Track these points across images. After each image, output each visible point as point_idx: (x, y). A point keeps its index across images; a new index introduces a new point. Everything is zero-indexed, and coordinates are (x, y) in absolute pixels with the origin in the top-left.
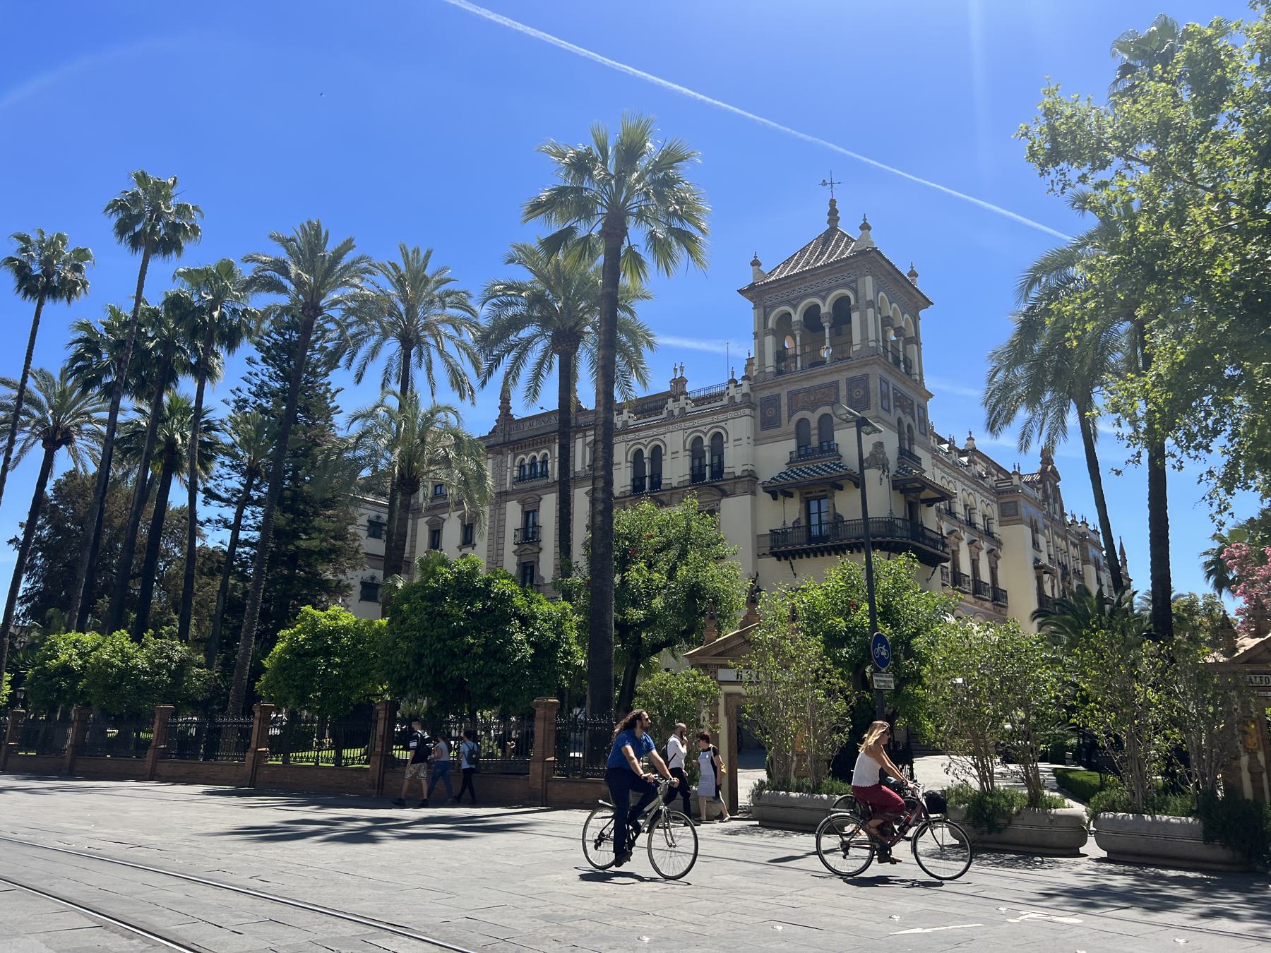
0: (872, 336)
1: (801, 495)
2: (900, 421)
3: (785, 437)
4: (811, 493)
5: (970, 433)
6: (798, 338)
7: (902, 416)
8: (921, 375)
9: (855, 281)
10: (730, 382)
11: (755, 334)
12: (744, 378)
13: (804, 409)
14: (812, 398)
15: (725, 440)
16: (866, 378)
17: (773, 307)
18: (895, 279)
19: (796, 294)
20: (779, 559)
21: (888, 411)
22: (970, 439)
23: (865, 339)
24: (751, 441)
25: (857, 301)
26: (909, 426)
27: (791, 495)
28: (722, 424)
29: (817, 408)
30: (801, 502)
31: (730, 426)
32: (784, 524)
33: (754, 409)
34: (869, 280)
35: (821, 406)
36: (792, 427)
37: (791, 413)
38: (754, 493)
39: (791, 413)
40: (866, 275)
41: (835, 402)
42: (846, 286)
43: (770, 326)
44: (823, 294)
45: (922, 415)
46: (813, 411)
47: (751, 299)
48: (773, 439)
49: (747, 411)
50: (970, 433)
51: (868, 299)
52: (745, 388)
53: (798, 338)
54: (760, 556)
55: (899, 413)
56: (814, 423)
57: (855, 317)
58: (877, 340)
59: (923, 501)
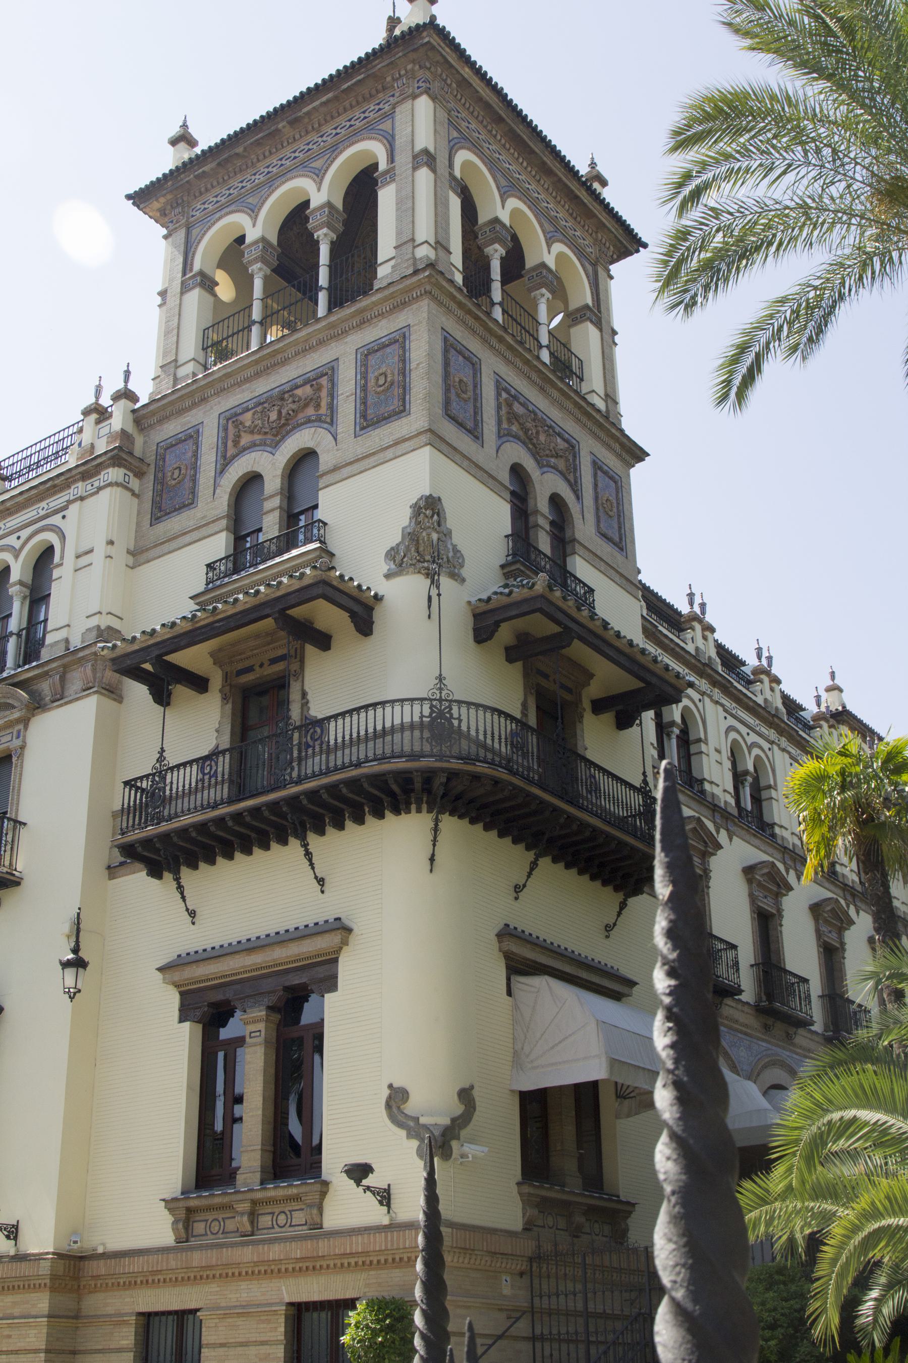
0: (424, 230)
1: (226, 677)
2: (517, 471)
3: (200, 531)
4: (249, 670)
5: (833, 675)
6: (258, 284)
7: (529, 464)
8: (611, 398)
9: (391, 115)
10: (86, 413)
11: (163, 294)
12: (116, 397)
13: (253, 446)
14: (273, 416)
15: (57, 559)
16: (400, 340)
17: (208, 219)
18: (512, 131)
19: (259, 178)
20: (155, 872)
21: (475, 433)
22: (835, 688)
23: (407, 242)
24: (119, 551)
25: (391, 158)
26: (556, 501)
27: (200, 684)
28: (56, 520)
29: (283, 439)
30: (225, 698)
31: (70, 523)
32: (161, 758)
33: (139, 475)
34: (424, 106)
35: (298, 426)
36: (222, 503)
37: (225, 462)
38: (113, 693)
39: (225, 462)
40: (415, 97)
41: (330, 420)
42: (369, 130)
43: (197, 266)
44: (318, 164)
45: (608, 493)
46: (276, 445)
47: (161, 217)
48: (174, 543)
49: (114, 474)
50: (833, 675)
51: (419, 147)
52: (118, 420)
53: (258, 284)
54: (112, 871)
55: (517, 453)
56: (273, 482)
57: (387, 198)
58: (441, 245)
59: (599, 706)
